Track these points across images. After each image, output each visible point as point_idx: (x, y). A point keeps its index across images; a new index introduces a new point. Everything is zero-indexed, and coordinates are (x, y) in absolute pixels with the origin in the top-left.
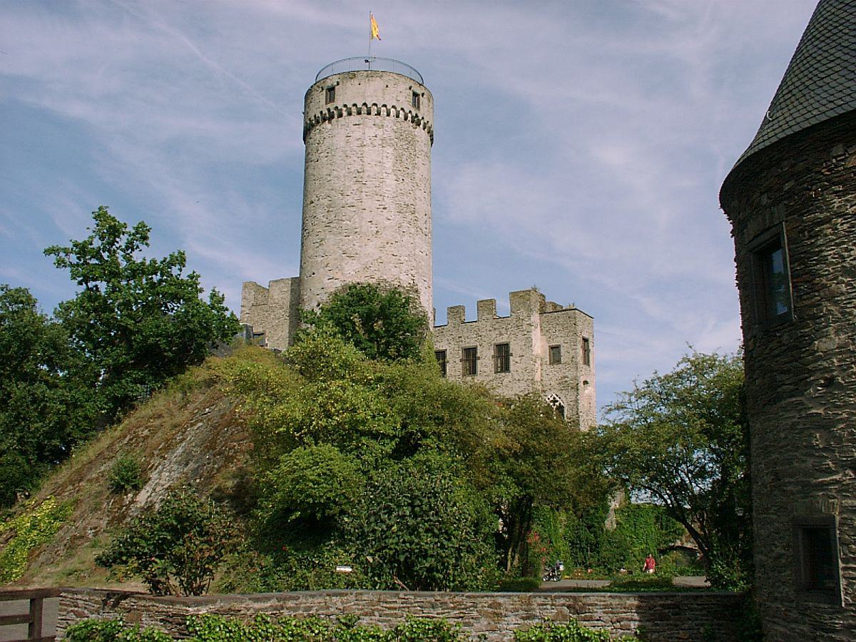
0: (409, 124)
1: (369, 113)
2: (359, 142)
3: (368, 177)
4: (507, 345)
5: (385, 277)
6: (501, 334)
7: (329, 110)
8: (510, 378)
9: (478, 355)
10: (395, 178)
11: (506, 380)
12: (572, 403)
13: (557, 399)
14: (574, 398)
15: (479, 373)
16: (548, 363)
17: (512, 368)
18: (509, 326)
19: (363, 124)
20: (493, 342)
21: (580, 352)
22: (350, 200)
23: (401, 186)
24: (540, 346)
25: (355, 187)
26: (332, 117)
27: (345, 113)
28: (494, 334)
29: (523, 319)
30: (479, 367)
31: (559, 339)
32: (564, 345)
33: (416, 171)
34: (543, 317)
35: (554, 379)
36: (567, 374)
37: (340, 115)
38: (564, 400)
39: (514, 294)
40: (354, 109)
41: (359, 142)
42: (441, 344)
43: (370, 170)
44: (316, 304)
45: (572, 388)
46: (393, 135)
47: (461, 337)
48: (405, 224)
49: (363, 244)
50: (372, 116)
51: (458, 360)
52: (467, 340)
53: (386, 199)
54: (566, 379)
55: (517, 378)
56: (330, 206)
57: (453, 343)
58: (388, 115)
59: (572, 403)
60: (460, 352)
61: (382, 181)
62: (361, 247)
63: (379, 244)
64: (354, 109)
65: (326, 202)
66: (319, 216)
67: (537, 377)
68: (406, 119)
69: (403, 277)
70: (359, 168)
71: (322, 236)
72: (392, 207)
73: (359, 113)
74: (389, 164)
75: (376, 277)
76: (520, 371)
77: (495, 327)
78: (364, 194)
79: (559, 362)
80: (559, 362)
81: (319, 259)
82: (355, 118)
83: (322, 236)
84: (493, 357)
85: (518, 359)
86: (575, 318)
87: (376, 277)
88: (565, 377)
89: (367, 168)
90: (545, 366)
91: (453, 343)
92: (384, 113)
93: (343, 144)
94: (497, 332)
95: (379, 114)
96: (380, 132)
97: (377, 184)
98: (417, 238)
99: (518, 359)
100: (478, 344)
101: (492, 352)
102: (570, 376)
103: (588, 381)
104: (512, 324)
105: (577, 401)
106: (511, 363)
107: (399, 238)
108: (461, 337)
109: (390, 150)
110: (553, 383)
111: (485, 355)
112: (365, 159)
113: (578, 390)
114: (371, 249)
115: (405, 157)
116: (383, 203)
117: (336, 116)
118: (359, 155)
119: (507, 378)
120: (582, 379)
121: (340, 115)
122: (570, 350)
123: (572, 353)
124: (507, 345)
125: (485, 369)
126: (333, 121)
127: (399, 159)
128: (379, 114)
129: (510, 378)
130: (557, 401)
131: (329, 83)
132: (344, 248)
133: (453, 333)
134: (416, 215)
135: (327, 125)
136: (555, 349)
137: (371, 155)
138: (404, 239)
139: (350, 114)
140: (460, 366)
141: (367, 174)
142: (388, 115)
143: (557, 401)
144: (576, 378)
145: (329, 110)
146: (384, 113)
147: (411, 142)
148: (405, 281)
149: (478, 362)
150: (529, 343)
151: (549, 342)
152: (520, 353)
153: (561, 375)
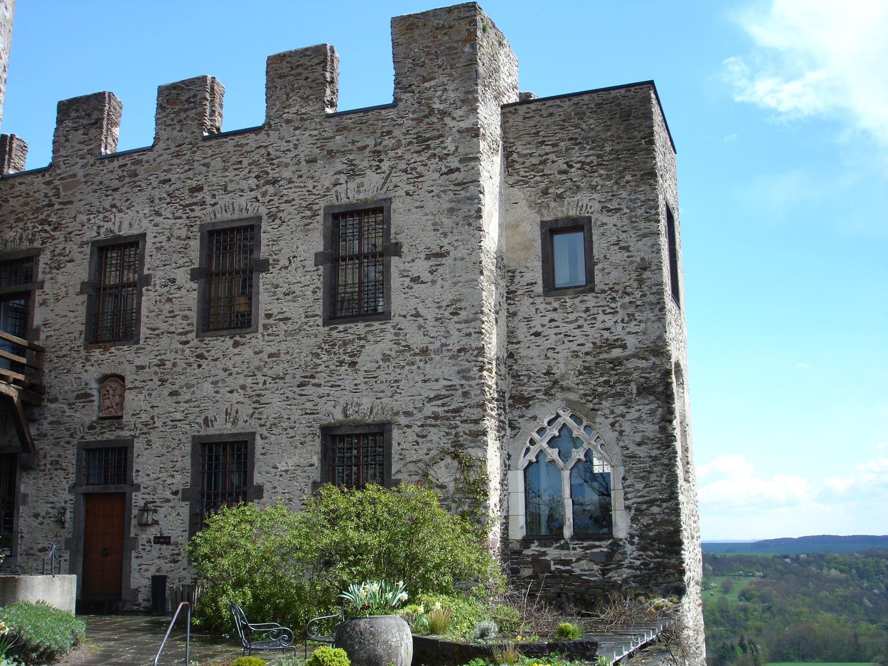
6: (353, 172)
8: (386, 345)
9: (264, 252)
12: (642, 451)
15: (262, 321)
16: (539, 288)
18: (388, 142)
20: (322, 204)
28: (325, 174)
29: (444, 113)
30: (265, 301)
31: (583, 198)
32: (604, 218)
34: (514, 120)
35: (564, 351)
39: (406, 28)
42: (127, 217)
45: (644, 390)
47: (199, 189)
51: (182, 276)
52: (223, 200)
54: (616, 353)
55: (417, 340)
57: (167, 212)
59: (642, 451)
60: (195, 244)
76: (430, 314)
77: (331, 145)
84: (319, 259)
85: (421, 268)
88: (612, 346)
90: (527, 301)
91: (167, 212)
94: (339, 164)
99: (421, 268)
100: (263, 211)
101: (316, 242)
102: (632, 342)
104: (397, 132)
106: (396, 282)
108: (199, 189)
111: (286, 253)
119: (376, 343)
122: (631, 240)
129: (386, 345)
130: (576, 442)
133: (173, 177)
140: (189, 296)
143: (576, 442)
149: (264, 281)
151: (539, 207)
152: (431, 241)
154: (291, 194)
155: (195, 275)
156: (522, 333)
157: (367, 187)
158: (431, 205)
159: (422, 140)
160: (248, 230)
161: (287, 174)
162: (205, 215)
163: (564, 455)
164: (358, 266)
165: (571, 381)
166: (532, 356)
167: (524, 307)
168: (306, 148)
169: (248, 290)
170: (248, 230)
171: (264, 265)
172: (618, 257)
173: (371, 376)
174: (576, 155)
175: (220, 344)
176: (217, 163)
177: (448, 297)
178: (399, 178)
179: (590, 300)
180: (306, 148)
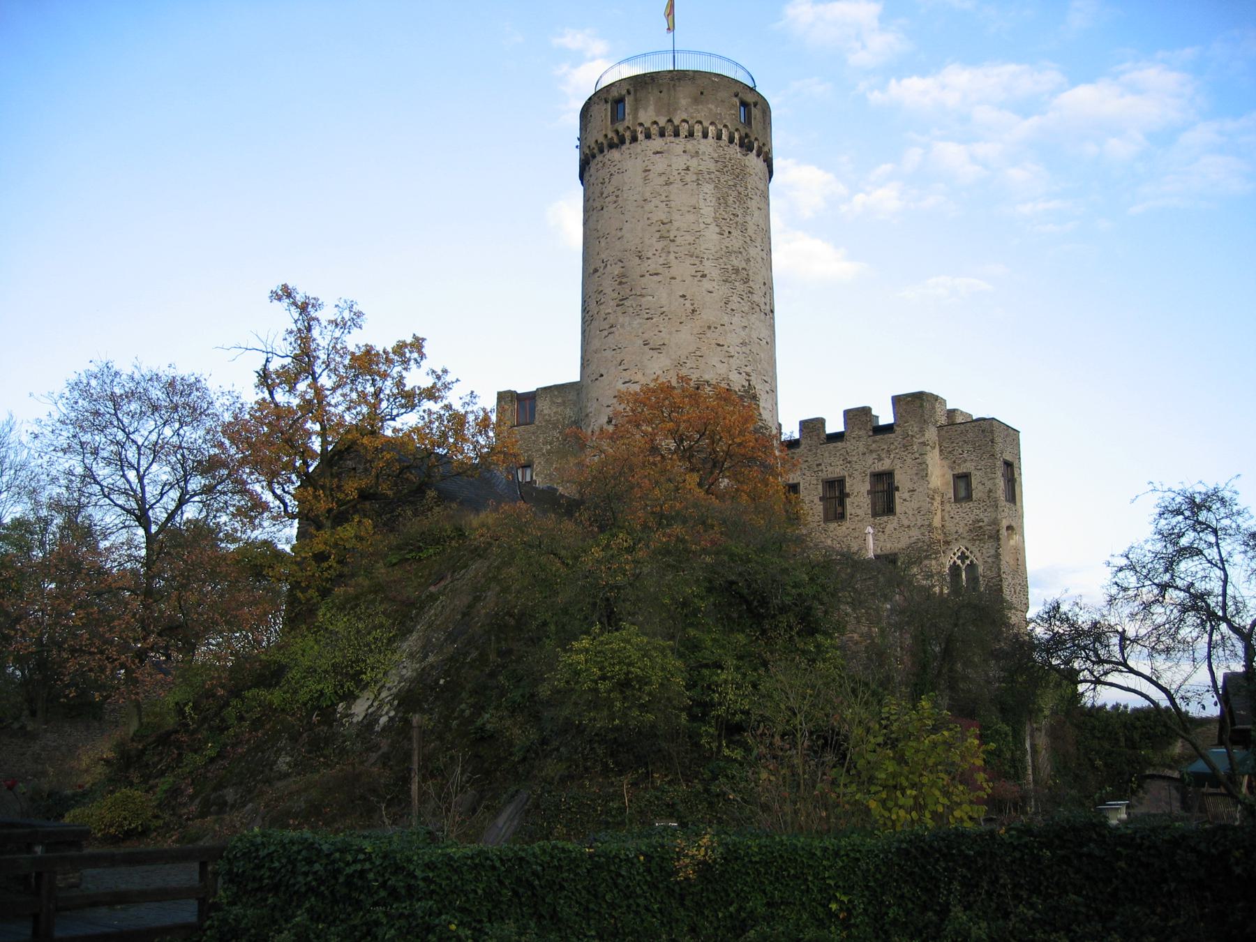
0: (735, 151)
1: (677, 134)
2: (664, 178)
3: (678, 229)
4: (889, 475)
5: (706, 377)
6: (880, 459)
7: (617, 132)
8: (895, 524)
9: (847, 490)
10: (717, 230)
11: (890, 528)
12: (989, 560)
13: (968, 553)
14: (993, 552)
17: (899, 508)
19: (668, 151)
20: (868, 472)
21: (1001, 483)
22: (652, 265)
23: (726, 242)
24: (939, 474)
25: (660, 245)
26: (622, 142)
27: (641, 137)
30: (849, 509)
31: (968, 464)
33: (748, 218)
36: (981, 516)
37: (634, 139)
38: (978, 555)
40: (654, 130)
41: (664, 178)
42: (791, 476)
43: (681, 222)
44: (606, 419)
45: (990, 537)
46: (712, 167)
48: (735, 298)
49: (673, 330)
50: (681, 139)
51: (816, 500)
52: (830, 469)
53: (705, 262)
55: (906, 523)
56: (624, 276)
58: (705, 136)
59: (989, 560)
60: (820, 487)
61: (698, 235)
62: (670, 333)
63: (695, 331)
64: (654, 130)
65: (617, 270)
66: (608, 291)
67: (937, 522)
68: (731, 140)
69: (734, 376)
70: (663, 217)
71: (611, 319)
72: (715, 274)
73: (662, 134)
74: (708, 211)
75: (694, 377)
76: (910, 513)
78: (672, 256)
79: (969, 497)
80: (969, 497)
81: (609, 354)
82: (657, 143)
83: (611, 319)
84: (869, 493)
85: (906, 495)
86: (992, 432)
87: (694, 377)
89: (676, 216)
92: (698, 134)
93: (639, 181)
94: (874, 456)
95: (691, 134)
96: (693, 163)
97: (690, 239)
98: (753, 318)
101: (868, 486)
102: (986, 520)
103: (1013, 524)
105: (997, 556)
106: (898, 501)
107: (726, 319)
109: (708, 188)
110: (960, 531)
112: (673, 204)
113: (998, 539)
114: (683, 339)
115: (731, 199)
116: (701, 268)
117: (628, 142)
118: (663, 198)
119: (891, 523)
120: (1005, 523)
121: (634, 139)
123: (989, 484)
124: (889, 475)
125: (860, 512)
126: (624, 147)
127: (722, 200)
128: (691, 134)
131: (615, 93)
132: (646, 336)
134: (751, 283)
135: (615, 154)
136: (963, 479)
137: (680, 197)
138: (735, 320)
139: (648, 136)
140: (819, 507)
141: (676, 224)
142: (705, 136)
144: (995, 522)
145: (617, 132)
146: (698, 134)
147: (741, 174)
148: (738, 382)
149: (848, 501)
150: (923, 474)
151: (952, 468)
152: (910, 485)
153: (973, 517)
154: (857, 467)
155: (821, 499)
156: (947, 517)
157: (885, 465)
158: (909, 471)
159: (905, 446)
160: (841, 482)
161: (855, 459)
162: (823, 475)
163: (963, 563)
164: (884, 493)
165: (965, 535)
166: (950, 526)
167: (947, 507)
168: (862, 449)
169: (842, 504)
170: (841, 482)
171: (848, 495)
172: (980, 487)
173: (890, 536)
174: (966, 447)
175: (833, 525)
176: (826, 454)
177: (916, 506)
178: (897, 462)
179: (971, 504)
180: (862, 449)
